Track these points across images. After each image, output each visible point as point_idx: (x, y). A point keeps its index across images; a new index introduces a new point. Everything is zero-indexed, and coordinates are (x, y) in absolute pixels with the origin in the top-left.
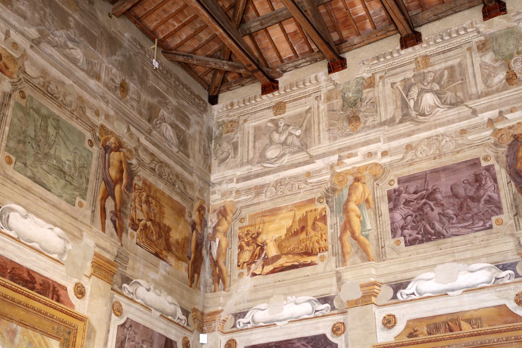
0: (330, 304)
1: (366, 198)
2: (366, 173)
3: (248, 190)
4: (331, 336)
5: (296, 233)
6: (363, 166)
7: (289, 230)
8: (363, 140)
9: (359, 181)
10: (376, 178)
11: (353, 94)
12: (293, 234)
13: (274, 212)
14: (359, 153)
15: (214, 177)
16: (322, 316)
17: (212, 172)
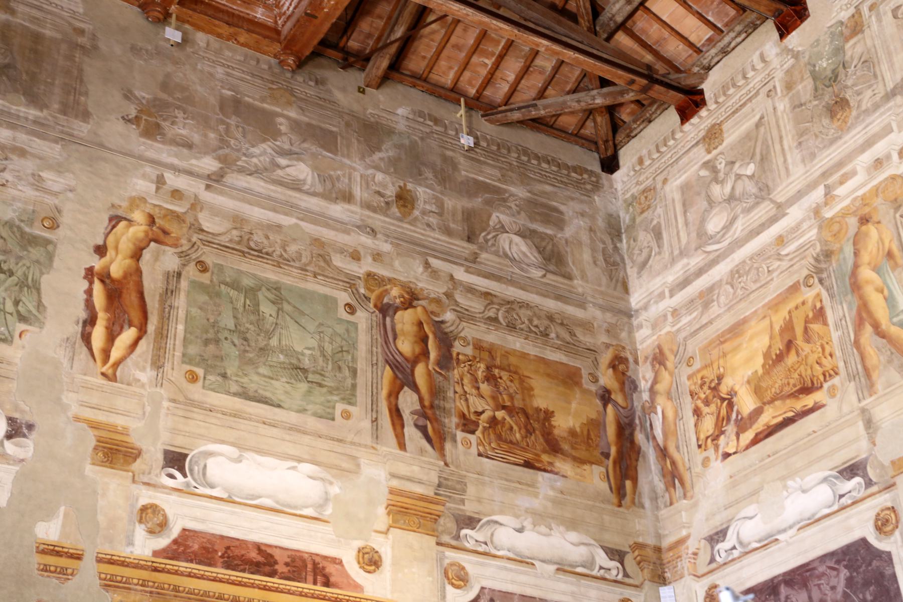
0: (863, 477)
1: (886, 250)
2: (878, 201)
3: (690, 303)
4: (876, 538)
5: (780, 358)
6: (870, 191)
7: (766, 355)
8: (861, 141)
9: (867, 221)
10: (897, 205)
11: (828, 60)
12: (775, 359)
13: (736, 330)
14: (859, 168)
15: (635, 300)
16: (853, 503)
17: (631, 290)
